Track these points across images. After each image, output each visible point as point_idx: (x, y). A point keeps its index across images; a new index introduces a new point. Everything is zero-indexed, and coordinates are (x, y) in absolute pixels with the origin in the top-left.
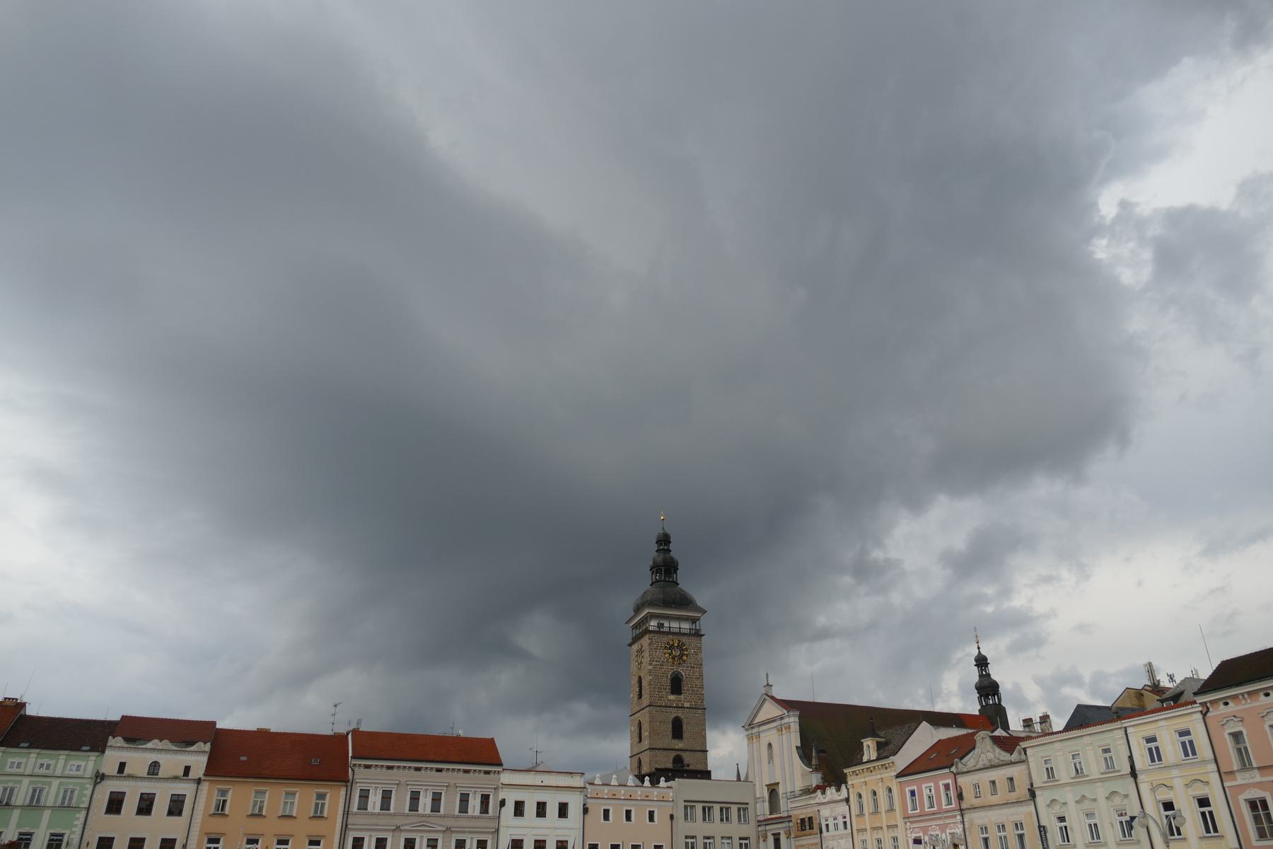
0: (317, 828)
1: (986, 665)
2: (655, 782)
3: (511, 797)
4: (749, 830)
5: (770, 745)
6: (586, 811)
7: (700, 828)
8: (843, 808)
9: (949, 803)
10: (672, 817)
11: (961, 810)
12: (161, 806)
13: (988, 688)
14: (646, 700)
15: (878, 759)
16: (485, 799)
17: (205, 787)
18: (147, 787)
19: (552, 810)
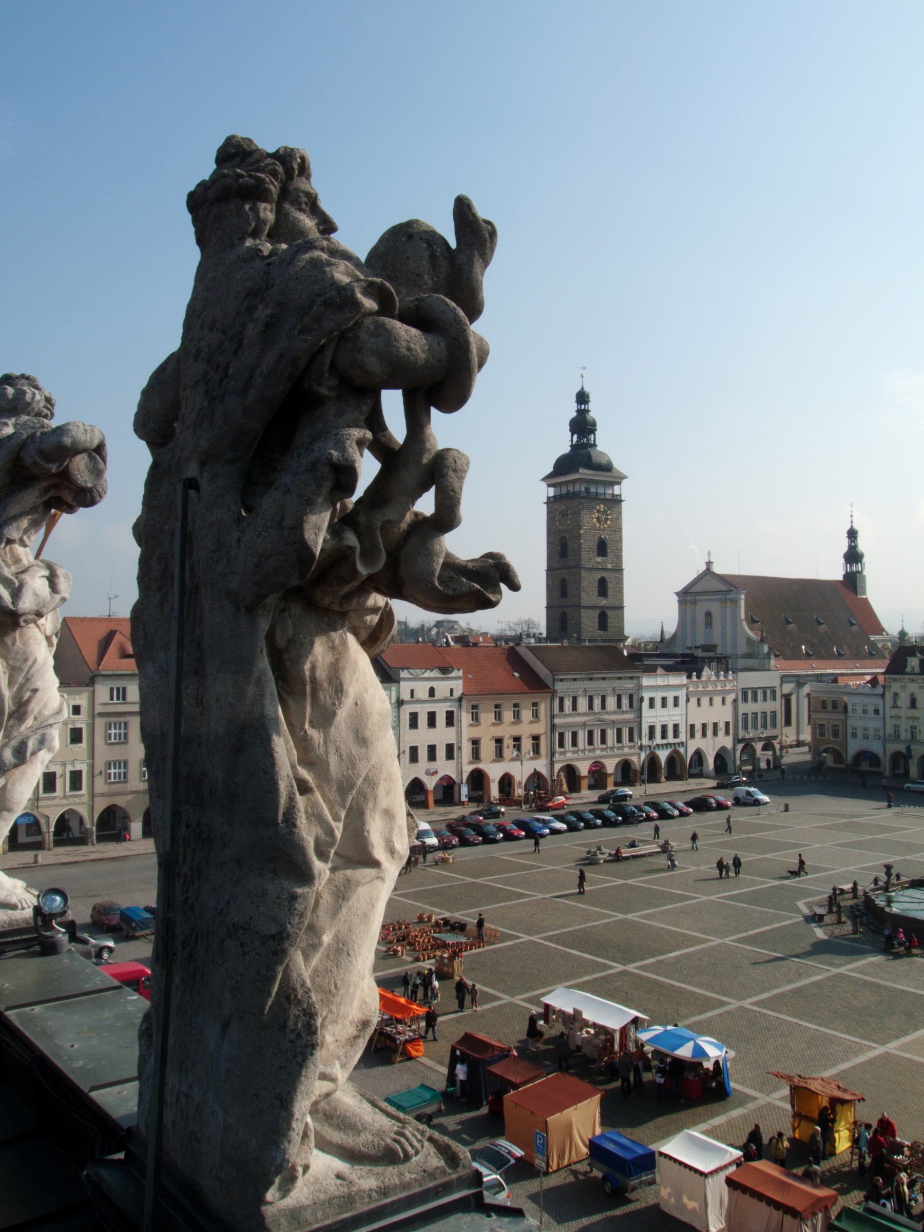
1: (855, 538)
5: (709, 615)
6: (688, 700)
7: (749, 707)
8: (879, 701)
12: (441, 719)
13: (853, 556)
16: (631, 697)
17: (464, 703)
18: (431, 707)
19: (670, 702)
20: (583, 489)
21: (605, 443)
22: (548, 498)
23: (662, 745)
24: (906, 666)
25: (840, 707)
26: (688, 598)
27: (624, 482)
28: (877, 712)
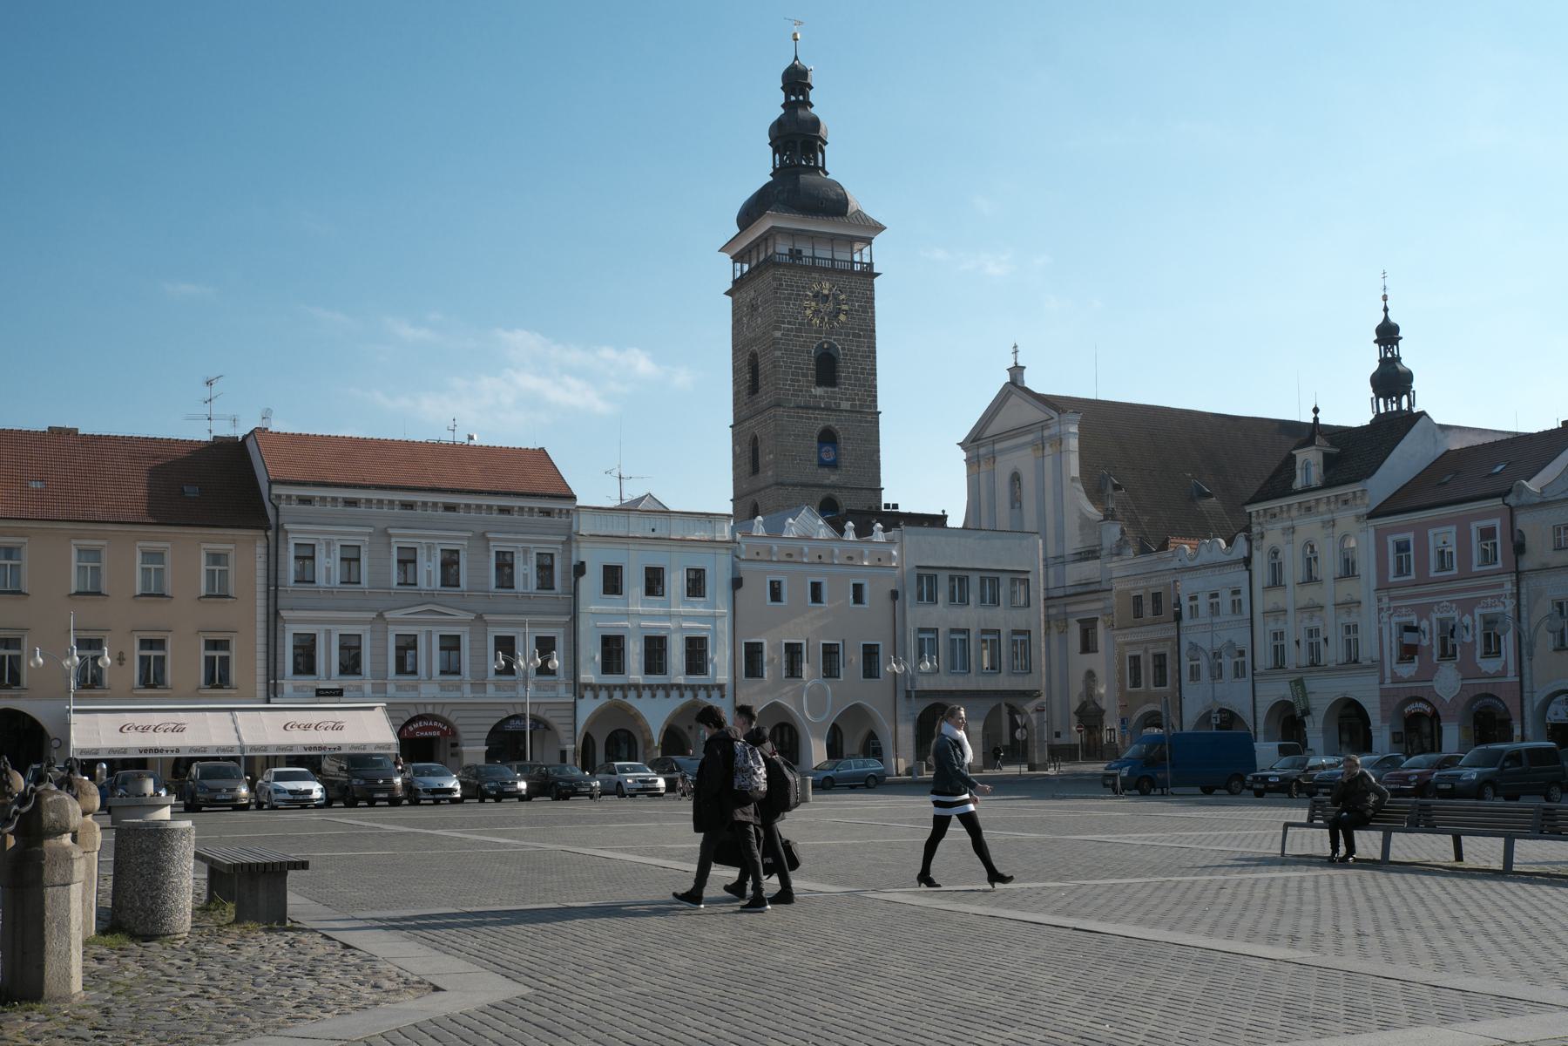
0: (218, 617)
2: (864, 531)
3: (595, 559)
4: (1035, 618)
5: (1016, 478)
6: (737, 583)
8: (1239, 577)
9: (1488, 557)
10: (894, 595)
11: (1518, 573)
14: (764, 398)
15: (1327, 485)
20: (783, 247)
21: (841, 163)
22: (735, 282)
23: (650, 687)
24: (1294, 476)
25: (1167, 605)
26: (982, 451)
27: (878, 240)
28: (1237, 606)
